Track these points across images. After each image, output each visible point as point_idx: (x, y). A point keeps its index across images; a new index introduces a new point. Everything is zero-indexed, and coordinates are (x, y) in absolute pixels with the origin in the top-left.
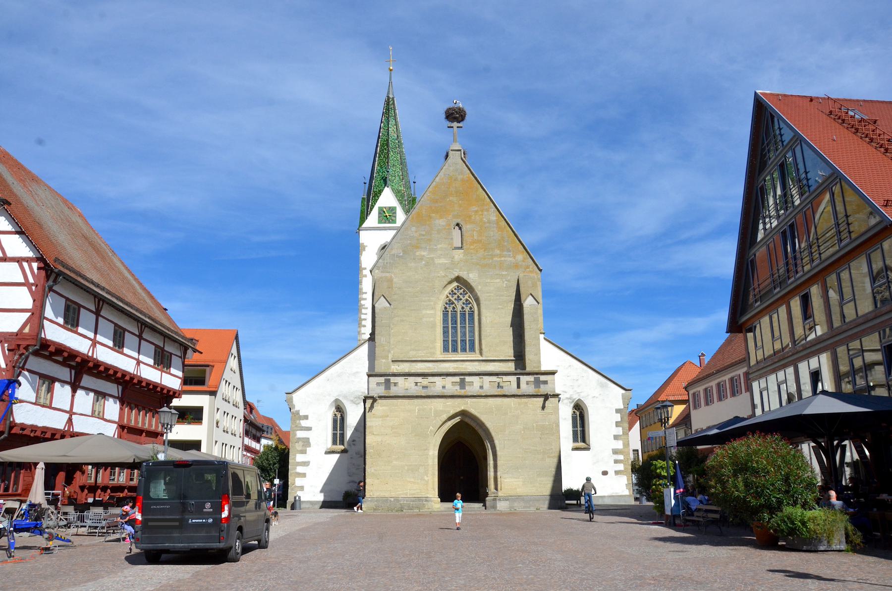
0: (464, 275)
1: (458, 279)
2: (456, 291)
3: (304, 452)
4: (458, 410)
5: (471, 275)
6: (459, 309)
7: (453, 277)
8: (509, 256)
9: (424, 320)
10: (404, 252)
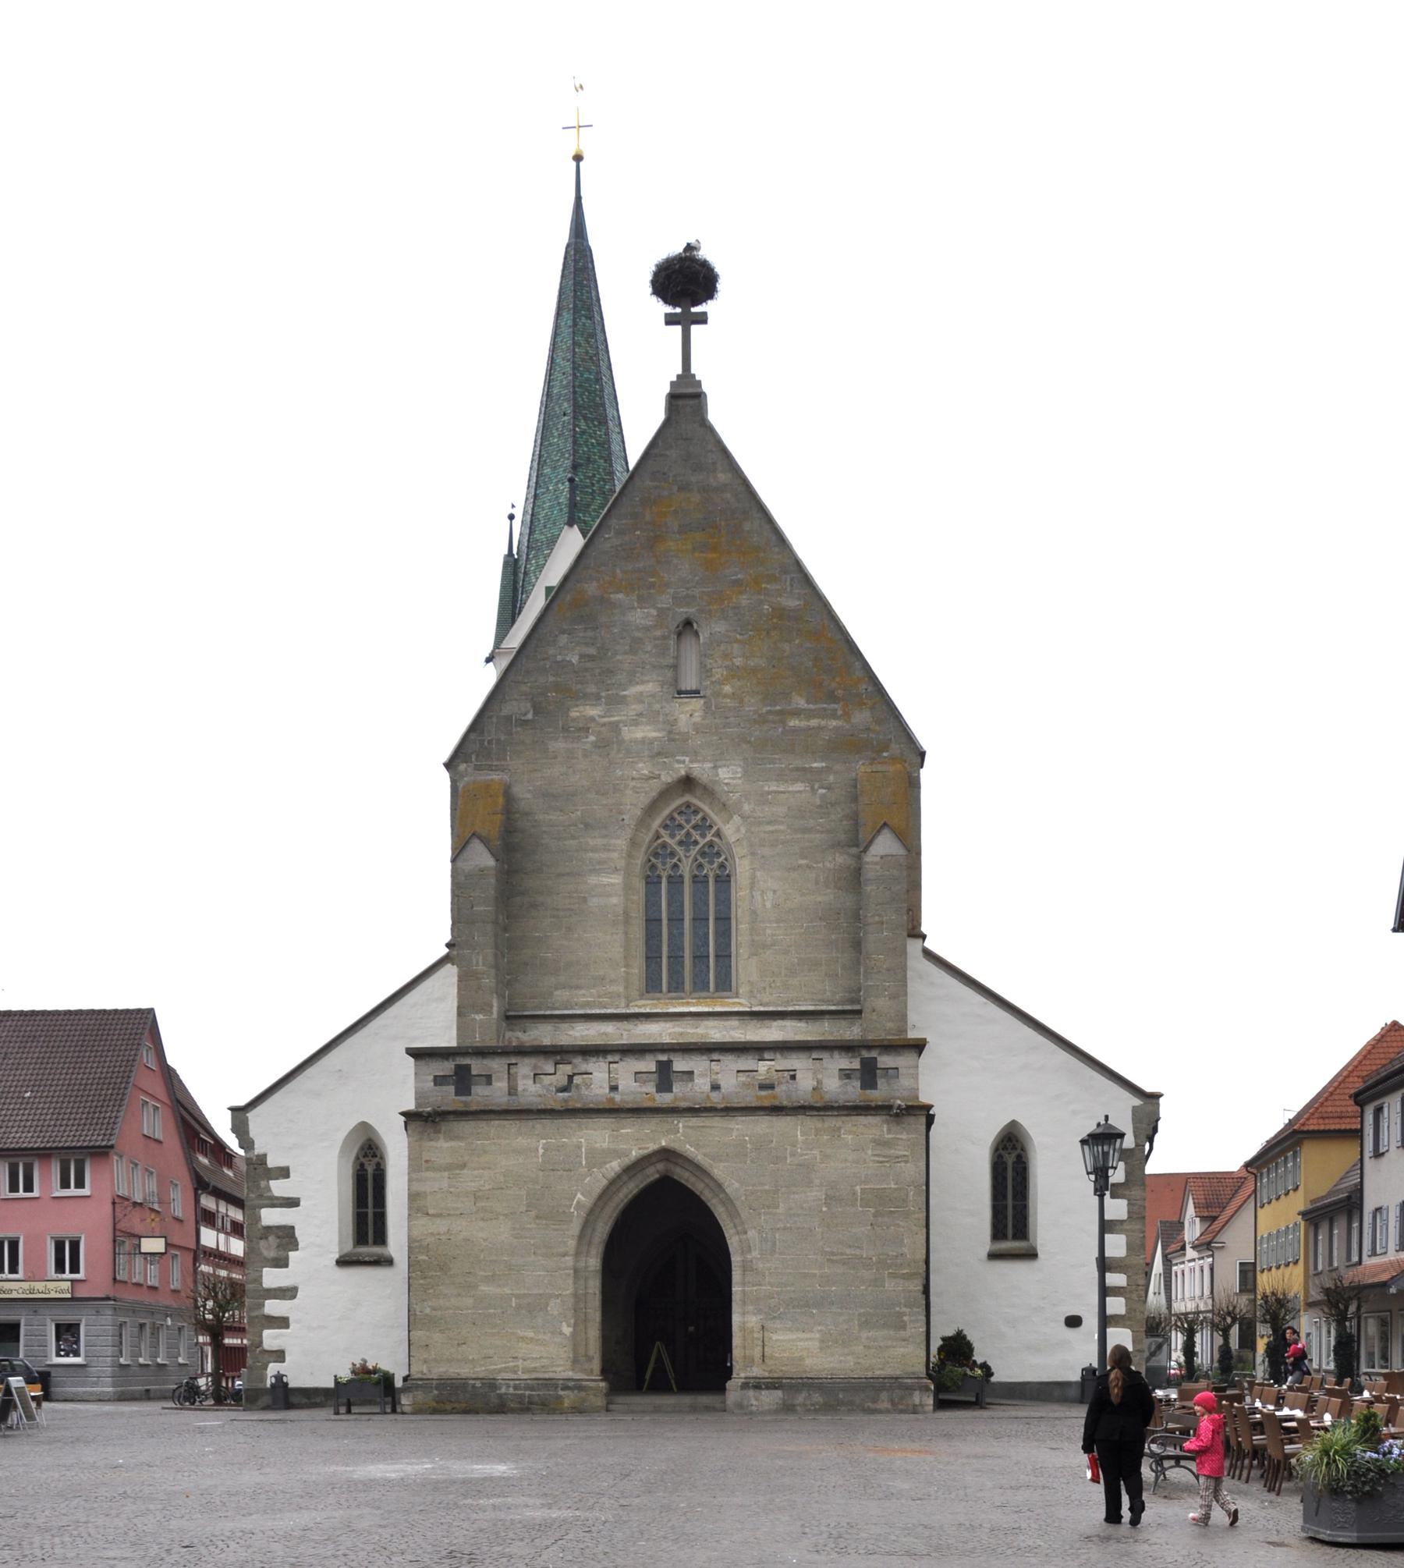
0: (701, 770)
1: (688, 783)
4: (652, 1147)
5: (724, 774)
6: (686, 870)
7: (667, 778)
9: (594, 902)
10: (537, 709)
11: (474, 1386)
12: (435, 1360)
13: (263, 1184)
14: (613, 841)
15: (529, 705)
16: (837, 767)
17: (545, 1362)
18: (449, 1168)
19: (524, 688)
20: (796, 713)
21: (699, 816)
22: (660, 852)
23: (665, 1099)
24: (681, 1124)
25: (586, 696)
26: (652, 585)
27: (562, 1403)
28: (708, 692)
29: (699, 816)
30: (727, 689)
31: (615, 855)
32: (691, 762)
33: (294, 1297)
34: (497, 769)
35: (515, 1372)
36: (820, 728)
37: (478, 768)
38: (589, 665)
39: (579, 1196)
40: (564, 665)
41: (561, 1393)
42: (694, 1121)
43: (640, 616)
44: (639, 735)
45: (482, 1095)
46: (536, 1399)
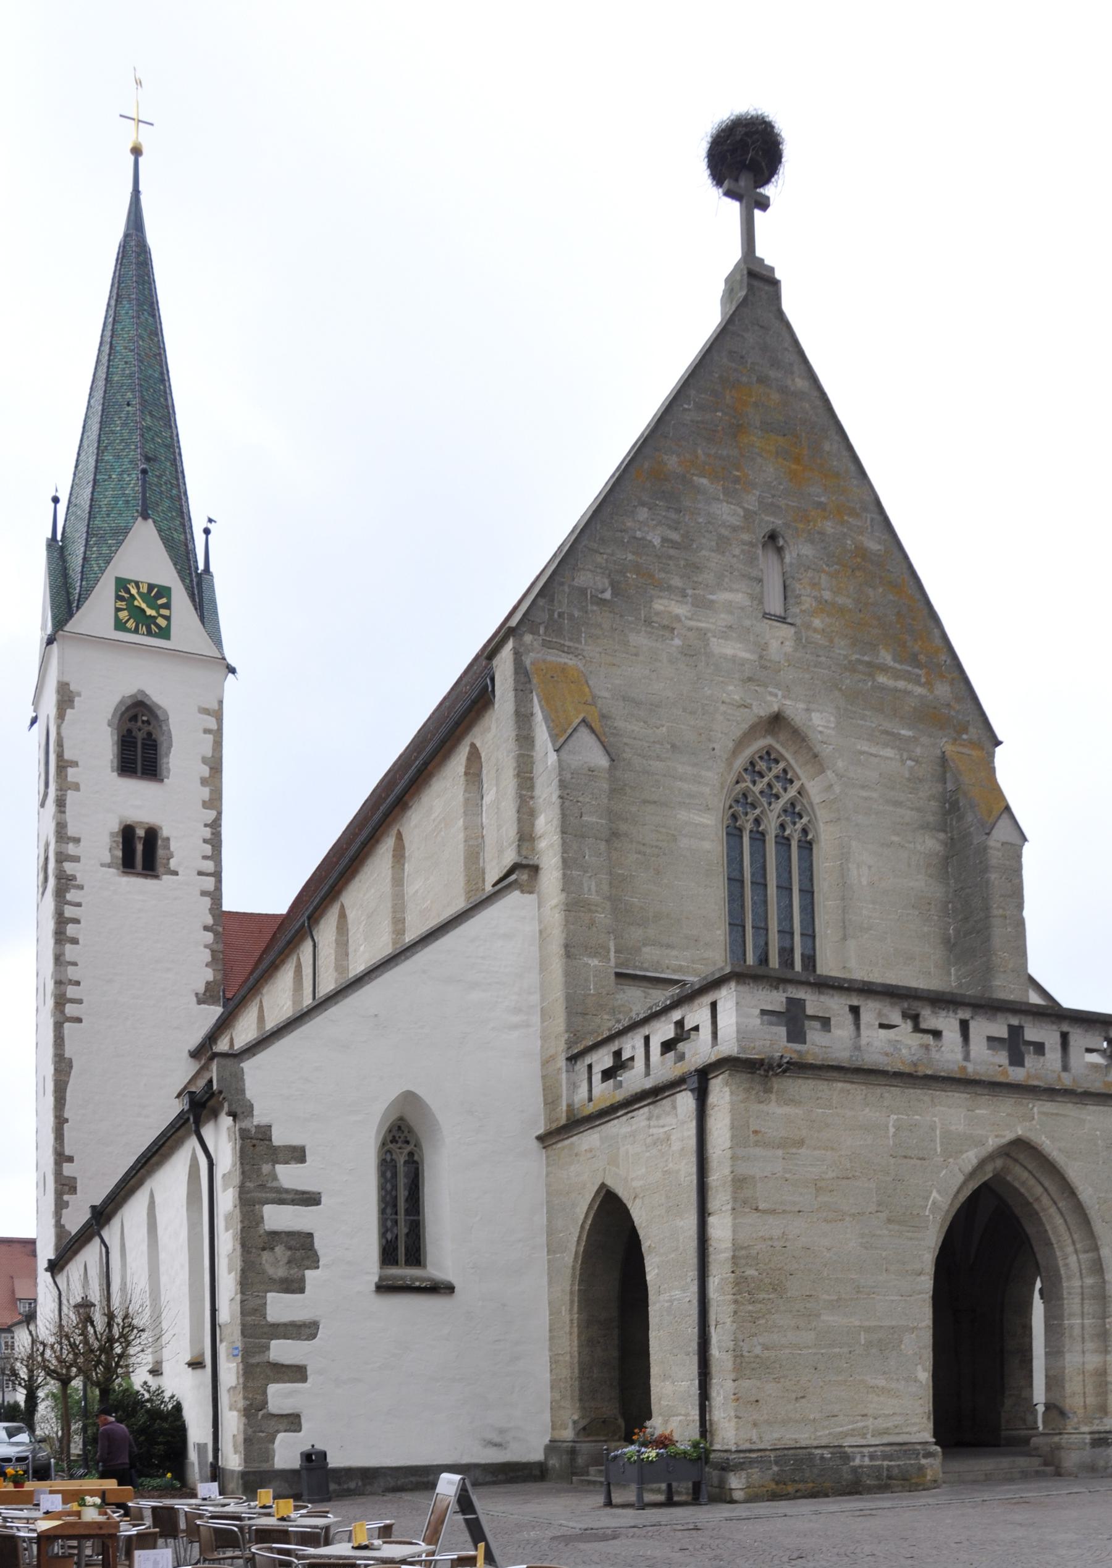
0: (795, 710)
1: (776, 722)
2: (762, 765)
3: (295, 1286)
4: (1009, 1136)
8: (918, 682)
9: (684, 842)
11: (822, 1458)
12: (768, 1422)
13: (266, 1168)
14: (703, 773)
15: (606, 581)
16: (924, 740)
17: (898, 1420)
18: (783, 1144)
19: (599, 559)
20: (884, 669)
21: (782, 765)
22: (744, 799)
23: (1017, 1075)
24: (1039, 1108)
25: (669, 588)
26: (737, 480)
27: (925, 1476)
28: (798, 622)
29: (782, 765)
30: (817, 623)
31: (707, 790)
32: (784, 697)
33: (314, 1336)
34: (569, 651)
35: (864, 1436)
36: (907, 693)
37: (546, 644)
38: (672, 552)
39: (935, 1194)
40: (642, 545)
41: (923, 1461)
42: (1049, 1107)
43: (727, 512)
44: (729, 651)
45: (819, 1044)
46: (896, 1471)
